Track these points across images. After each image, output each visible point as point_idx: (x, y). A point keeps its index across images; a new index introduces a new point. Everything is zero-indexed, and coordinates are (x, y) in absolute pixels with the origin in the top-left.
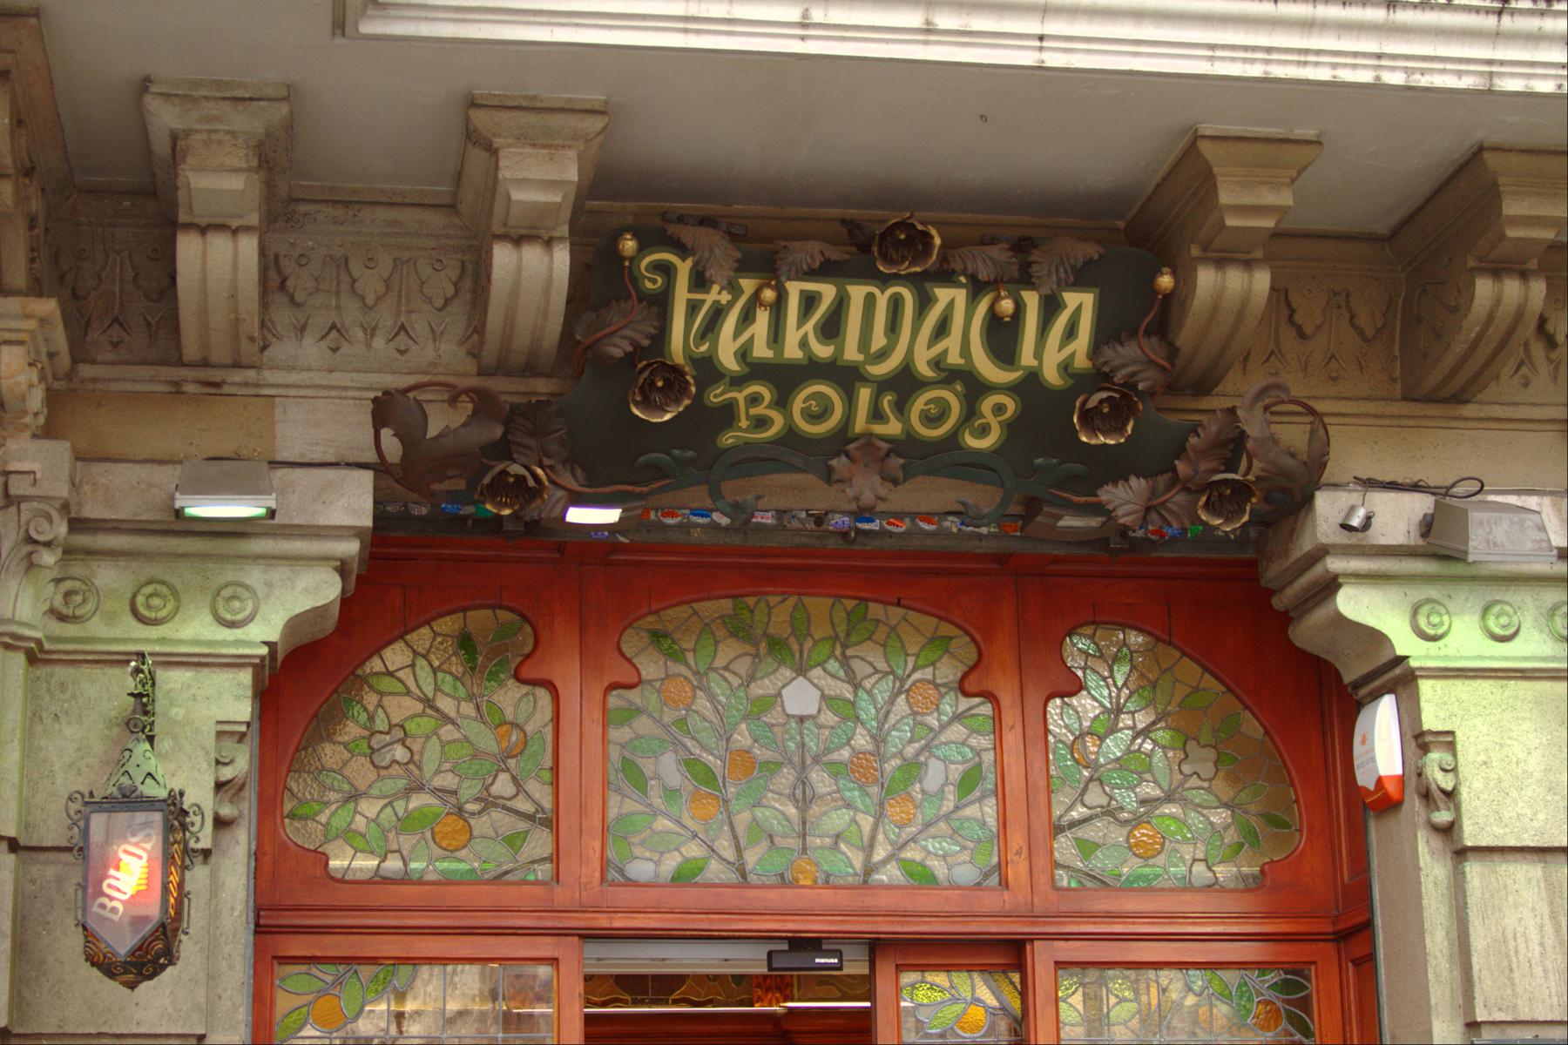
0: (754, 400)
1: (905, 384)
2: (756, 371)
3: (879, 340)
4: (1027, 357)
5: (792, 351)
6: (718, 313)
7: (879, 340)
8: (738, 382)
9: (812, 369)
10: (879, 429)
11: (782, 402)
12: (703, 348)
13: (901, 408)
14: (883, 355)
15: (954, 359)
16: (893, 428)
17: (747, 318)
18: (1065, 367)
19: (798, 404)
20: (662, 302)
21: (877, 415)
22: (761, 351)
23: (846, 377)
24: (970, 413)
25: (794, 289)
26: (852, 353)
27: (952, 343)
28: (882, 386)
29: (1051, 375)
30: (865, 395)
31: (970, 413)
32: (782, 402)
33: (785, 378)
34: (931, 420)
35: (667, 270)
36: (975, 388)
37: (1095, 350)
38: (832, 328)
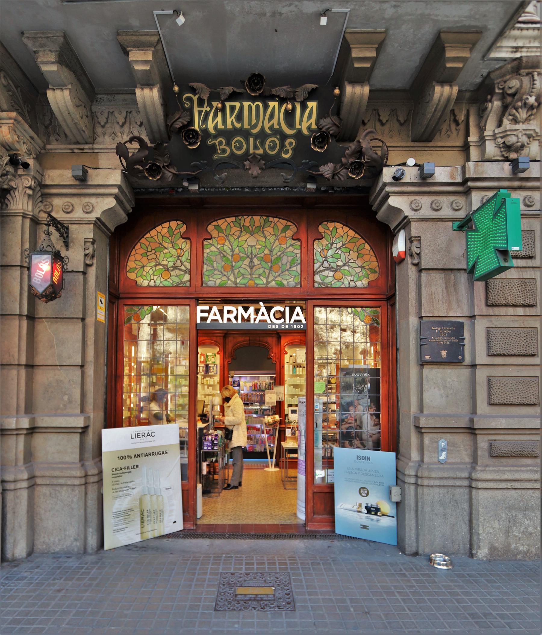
0: (220, 143)
1: (262, 136)
2: (220, 133)
3: (254, 121)
4: (298, 126)
5: (229, 126)
6: (207, 114)
7: (254, 121)
8: (215, 137)
9: (235, 132)
10: (257, 152)
11: (228, 144)
12: (204, 126)
13: (263, 144)
14: (255, 126)
15: (276, 126)
16: (261, 151)
17: (215, 116)
18: (309, 128)
19: (233, 144)
20: (191, 111)
21: (256, 147)
22: (221, 126)
23: (246, 134)
24: (283, 146)
25: (228, 104)
26: (246, 126)
27: (275, 121)
28: (256, 137)
29: (305, 132)
30: (251, 140)
31: (283, 146)
32: (228, 144)
33: (228, 135)
34: (272, 148)
35: (190, 99)
36: (284, 137)
37: (317, 123)
38: (239, 118)
